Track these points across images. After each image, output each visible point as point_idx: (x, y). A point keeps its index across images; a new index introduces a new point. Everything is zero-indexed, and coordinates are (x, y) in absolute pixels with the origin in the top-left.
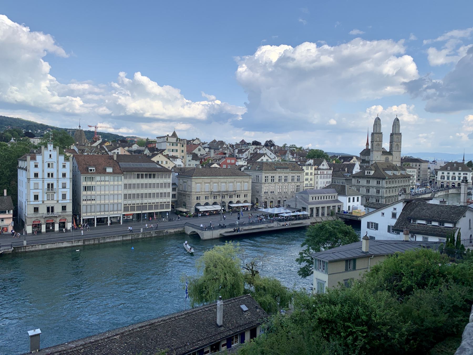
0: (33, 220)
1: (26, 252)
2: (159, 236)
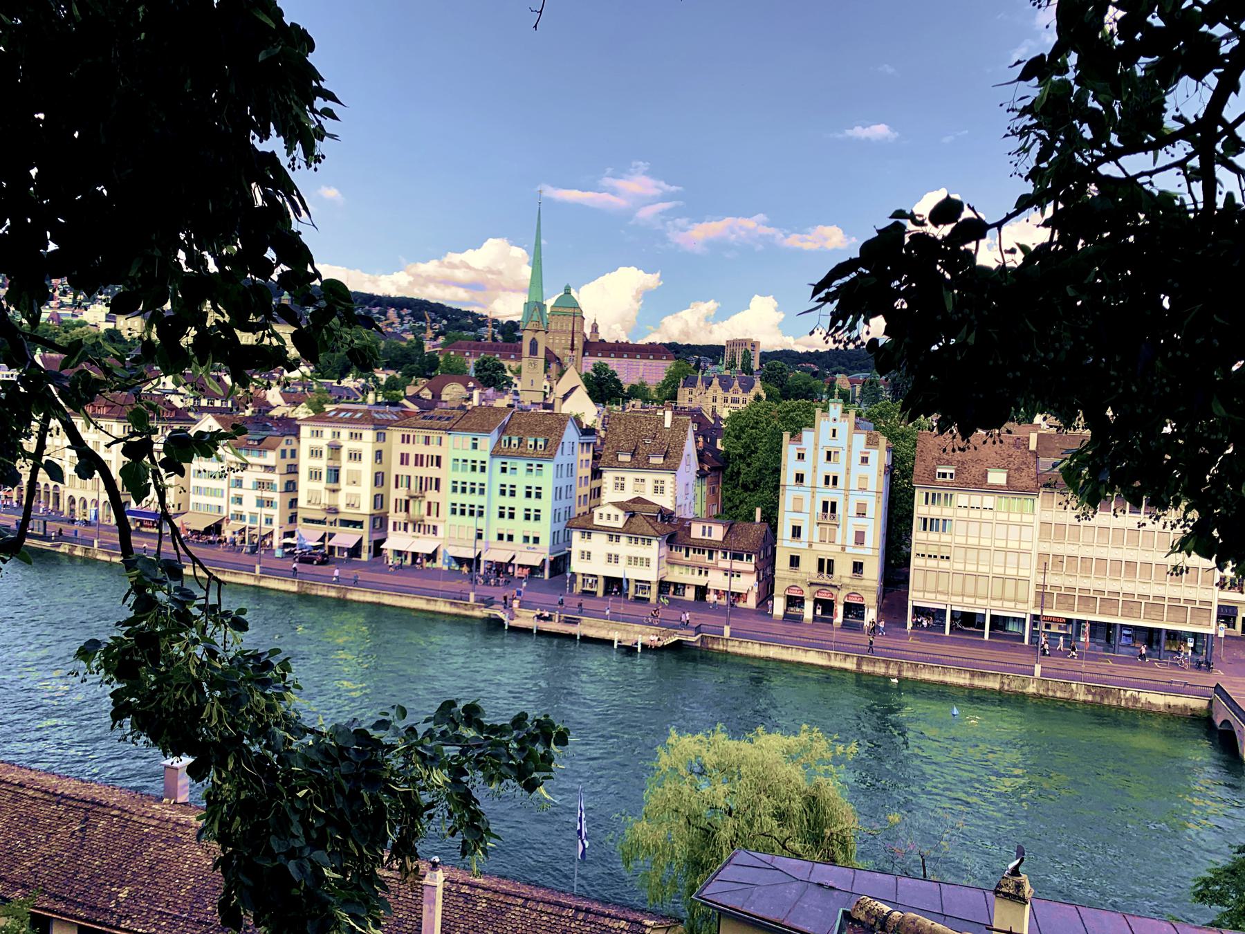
0: (788, 584)
1: (727, 653)
2: (1102, 706)
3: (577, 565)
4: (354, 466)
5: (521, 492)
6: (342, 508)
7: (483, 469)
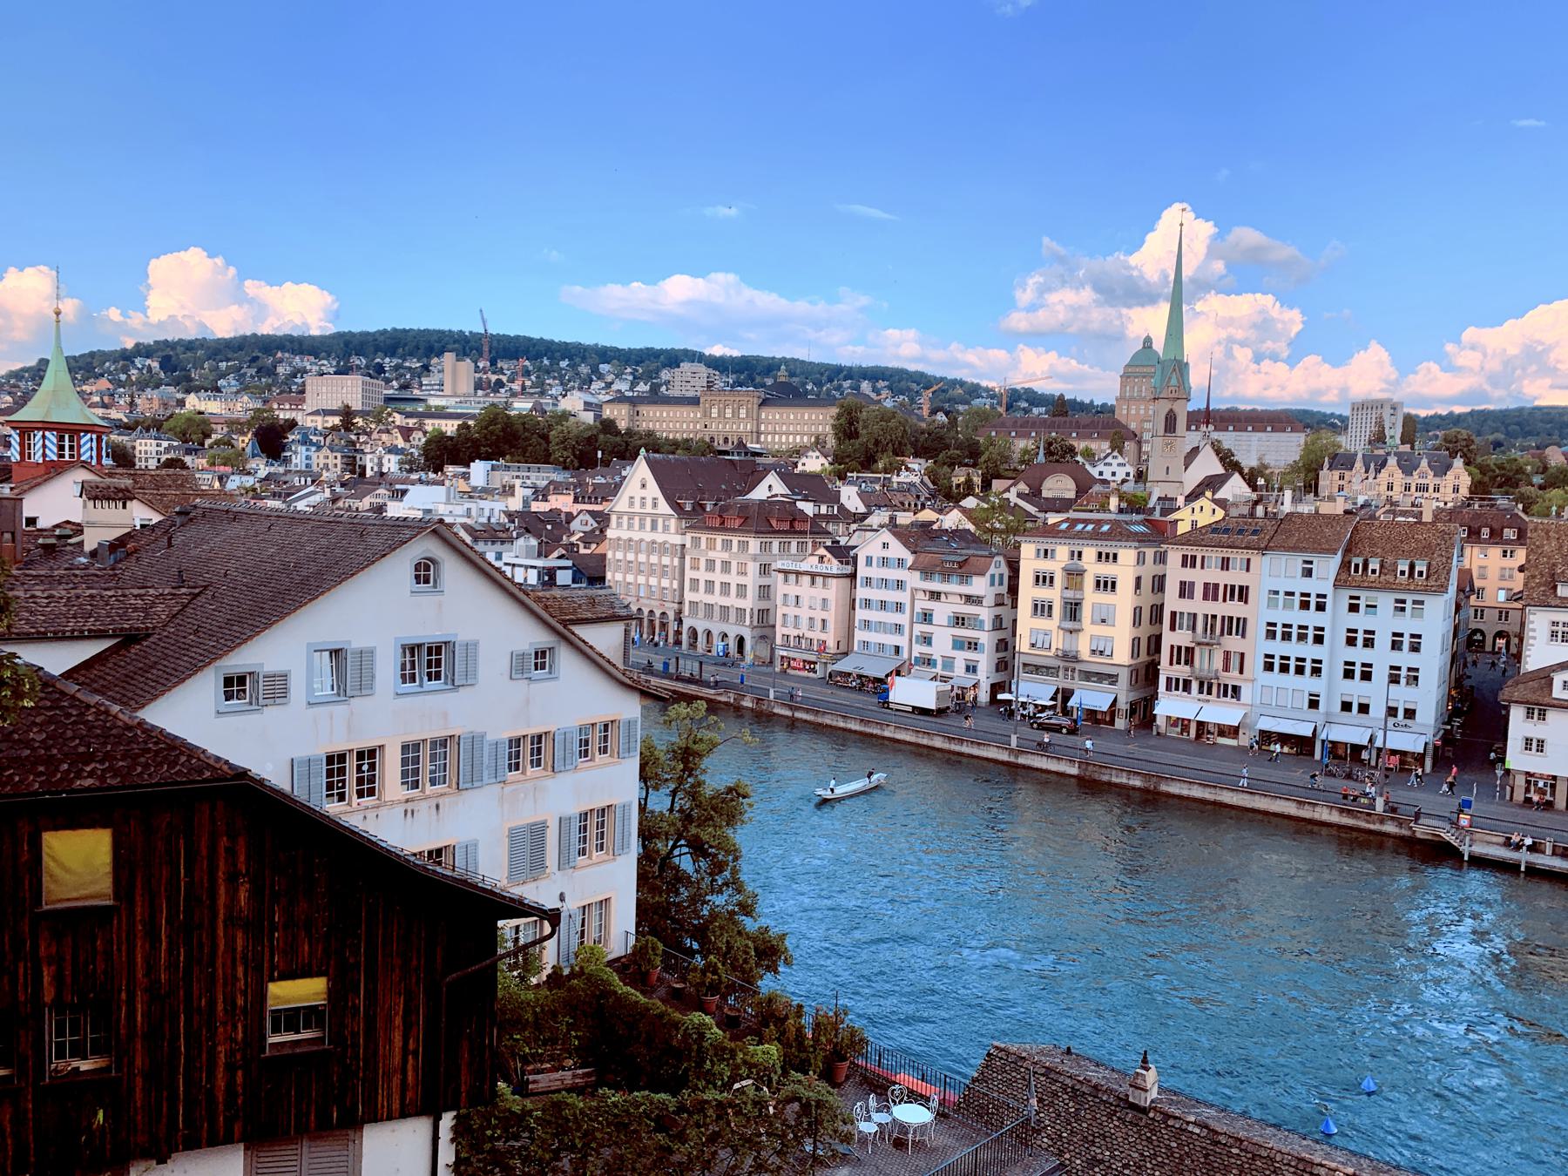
3: (1517, 758)
4: (1104, 598)
5: (1383, 640)
6: (1085, 654)
7: (1321, 607)
